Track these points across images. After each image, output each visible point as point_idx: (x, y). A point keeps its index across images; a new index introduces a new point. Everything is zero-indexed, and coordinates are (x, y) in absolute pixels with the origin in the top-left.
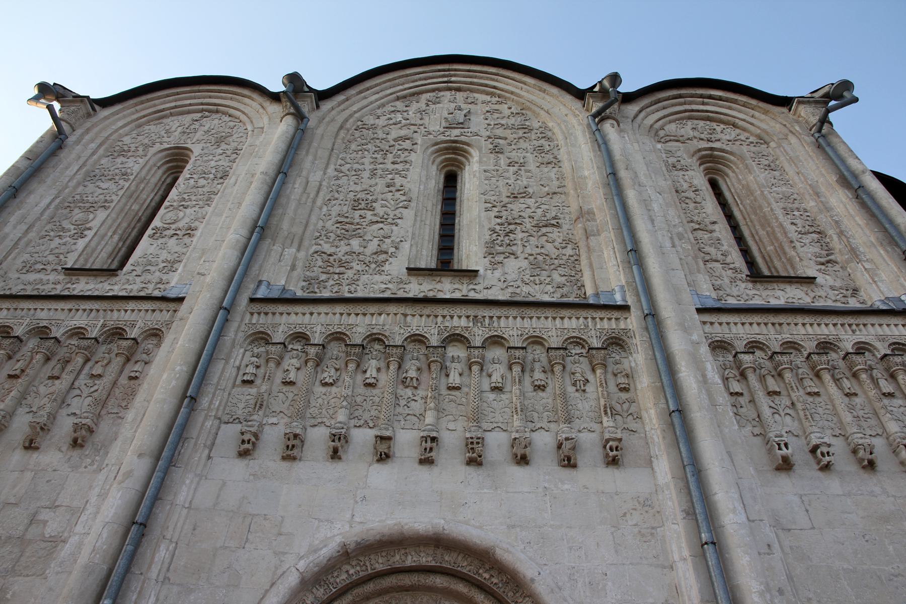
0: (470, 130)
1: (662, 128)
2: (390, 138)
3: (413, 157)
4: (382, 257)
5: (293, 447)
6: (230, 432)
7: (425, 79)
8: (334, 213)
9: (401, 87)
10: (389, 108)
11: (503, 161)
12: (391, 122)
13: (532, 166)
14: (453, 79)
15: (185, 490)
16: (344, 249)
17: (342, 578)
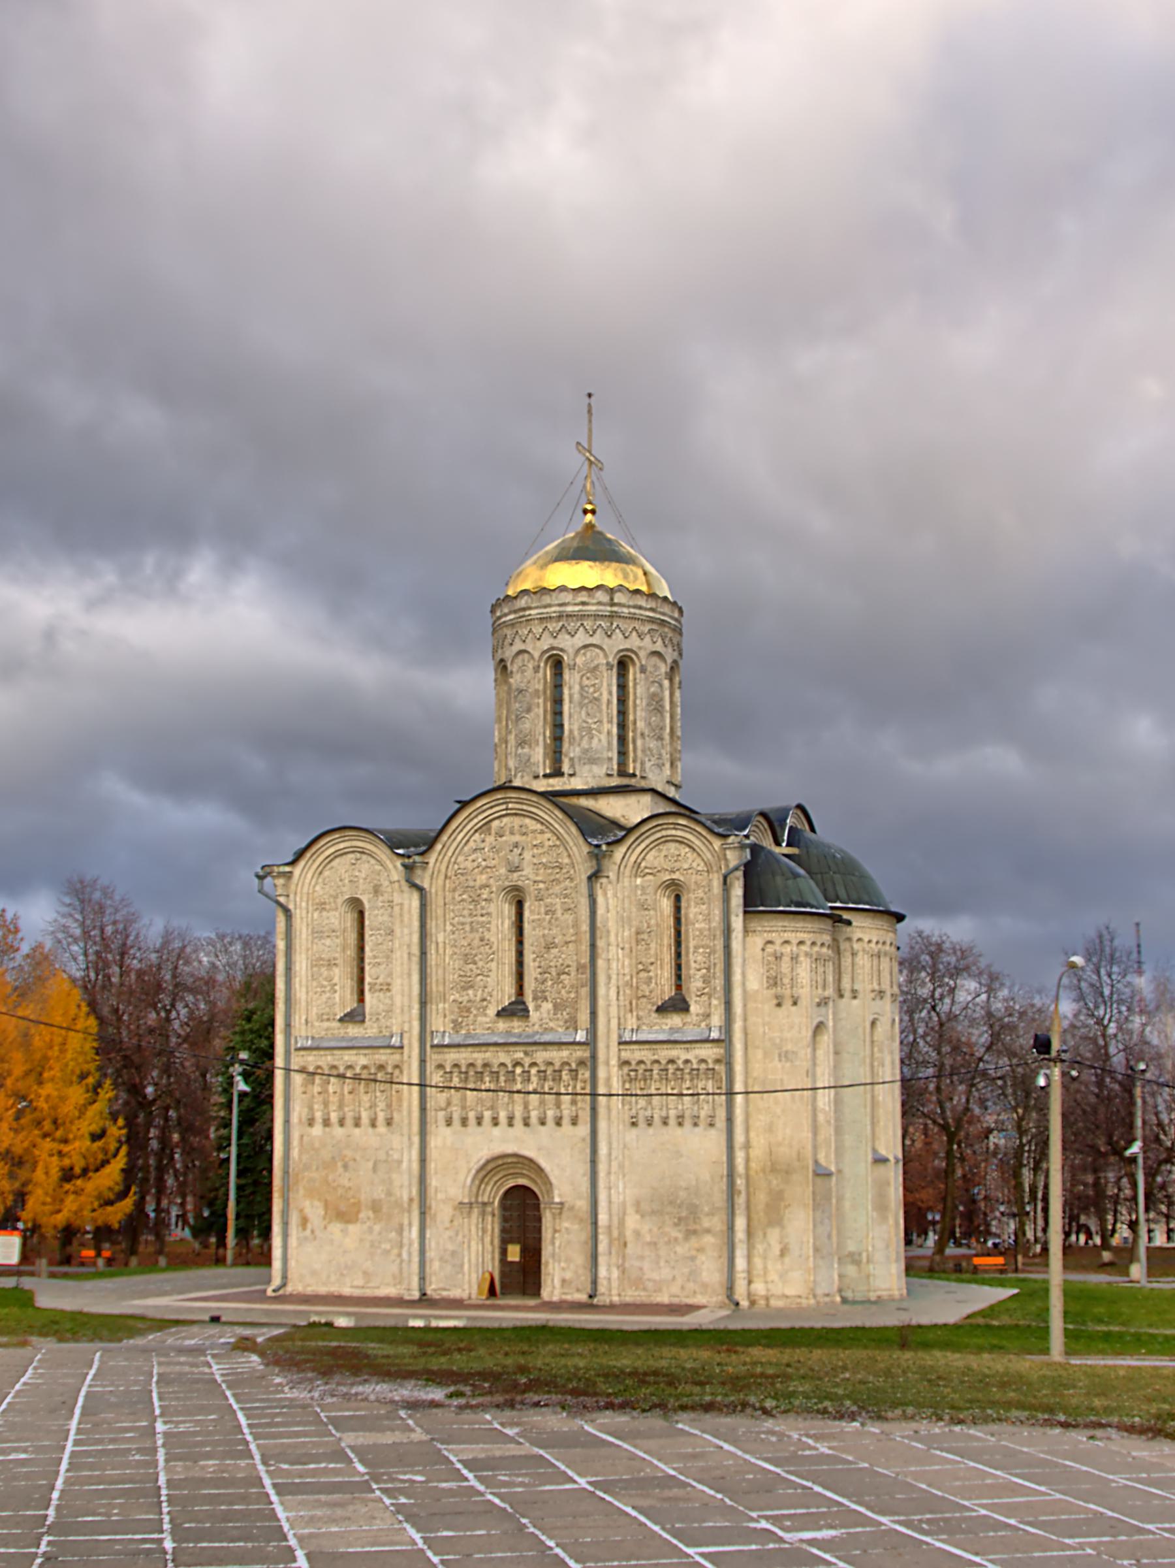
0: (524, 873)
1: (644, 859)
2: (478, 883)
3: (492, 908)
4: (485, 1003)
5: (464, 1122)
6: (441, 1114)
7: (491, 807)
8: (456, 966)
9: (476, 821)
10: (472, 844)
11: (543, 910)
12: (475, 864)
13: (559, 912)
14: (510, 806)
15: (434, 1142)
16: (466, 998)
17: (489, 1167)
